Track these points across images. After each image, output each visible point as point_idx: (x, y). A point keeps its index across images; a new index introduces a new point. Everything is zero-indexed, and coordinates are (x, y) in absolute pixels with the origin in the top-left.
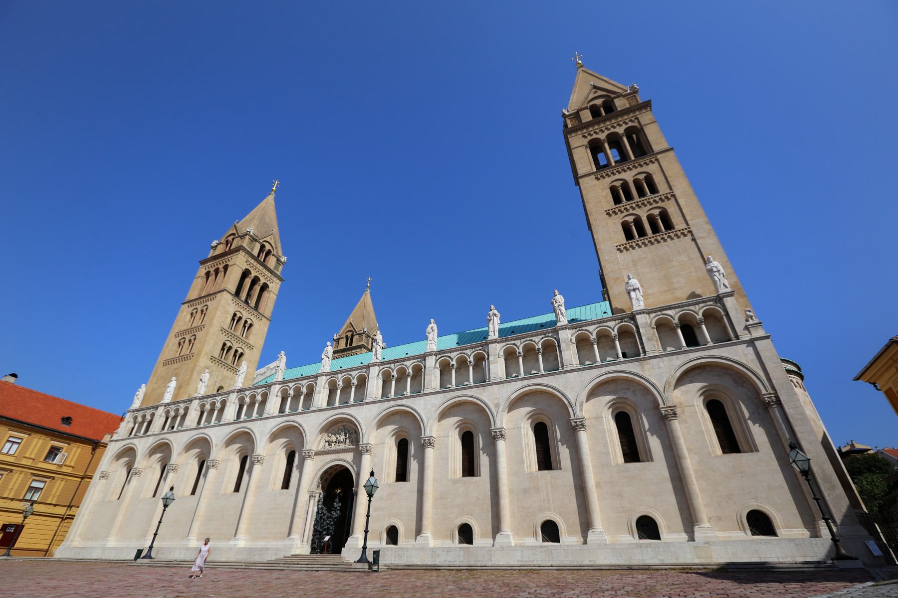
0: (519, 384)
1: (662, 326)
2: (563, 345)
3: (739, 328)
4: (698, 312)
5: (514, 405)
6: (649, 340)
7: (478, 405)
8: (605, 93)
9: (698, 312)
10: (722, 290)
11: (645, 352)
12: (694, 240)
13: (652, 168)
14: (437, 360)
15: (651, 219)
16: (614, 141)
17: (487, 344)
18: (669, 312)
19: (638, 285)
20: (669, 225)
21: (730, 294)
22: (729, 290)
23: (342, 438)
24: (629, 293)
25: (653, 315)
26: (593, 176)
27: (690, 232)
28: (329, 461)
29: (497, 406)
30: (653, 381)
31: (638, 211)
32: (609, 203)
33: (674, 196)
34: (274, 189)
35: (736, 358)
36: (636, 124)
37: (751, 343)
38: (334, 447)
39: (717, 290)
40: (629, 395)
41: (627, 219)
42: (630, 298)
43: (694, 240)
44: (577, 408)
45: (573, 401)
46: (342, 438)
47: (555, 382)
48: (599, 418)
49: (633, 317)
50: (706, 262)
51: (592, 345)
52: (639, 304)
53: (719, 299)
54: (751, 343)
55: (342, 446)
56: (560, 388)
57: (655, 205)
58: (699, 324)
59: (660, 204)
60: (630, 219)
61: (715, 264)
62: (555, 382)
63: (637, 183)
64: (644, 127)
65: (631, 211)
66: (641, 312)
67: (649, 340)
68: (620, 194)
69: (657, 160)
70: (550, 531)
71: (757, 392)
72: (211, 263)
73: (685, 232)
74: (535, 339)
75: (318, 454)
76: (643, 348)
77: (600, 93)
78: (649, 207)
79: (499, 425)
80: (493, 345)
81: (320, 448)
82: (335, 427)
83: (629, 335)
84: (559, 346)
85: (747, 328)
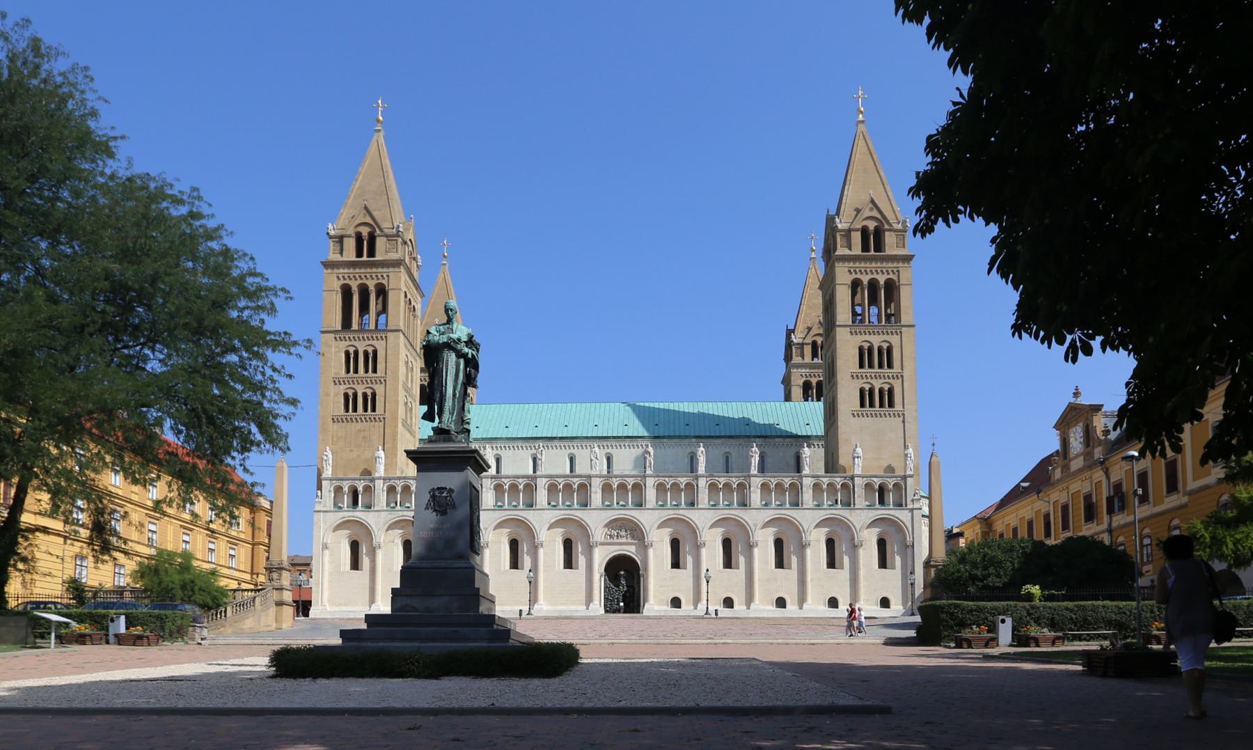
0: (772, 512)
1: (868, 486)
2: (804, 489)
3: (909, 500)
4: (891, 483)
5: (766, 525)
6: (859, 496)
7: (739, 521)
8: (880, 217)
9: (891, 483)
10: (909, 472)
11: (854, 504)
12: (904, 422)
13: (894, 340)
14: (707, 482)
15: (881, 391)
16: (873, 285)
17: (750, 476)
18: (874, 479)
19: (861, 455)
20: (891, 405)
21: (911, 476)
22: (912, 473)
23: (623, 533)
24: (854, 458)
25: (865, 479)
26: (848, 329)
27: (903, 415)
28: (614, 551)
29: (756, 525)
30: (855, 524)
31: (874, 382)
32: (854, 366)
33: (902, 376)
34: (381, 118)
35: (901, 518)
36: (895, 277)
37: (912, 510)
38: (616, 540)
39: (905, 472)
40: (839, 530)
41: (865, 386)
42: (854, 464)
43: (904, 422)
44: (808, 534)
45: (806, 530)
46: (623, 533)
47: (795, 514)
48: (818, 541)
49: (852, 478)
50: (906, 447)
51: (823, 491)
52: (858, 471)
53: (905, 478)
54: (912, 510)
55: (624, 540)
56: (799, 520)
57: (887, 380)
58: (889, 492)
59: (891, 381)
60: (867, 387)
61: (910, 451)
62: (795, 514)
63: (880, 350)
64: (901, 287)
65: (869, 380)
66: (859, 476)
67: (859, 496)
68: (866, 357)
69: (901, 332)
70: (781, 603)
71: (905, 538)
72: (346, 271)
73: (901, 413)
74: (785, 479)
75: (602, 544)
76: (854, 501)
77: (875, 214)
78: (883, 381)
79: (756, 538)
80: (755, 478)
81: (603, 540)
82: (614, 524)
83: (848, 489)
84: (802, 489)
85: (913, 501)
